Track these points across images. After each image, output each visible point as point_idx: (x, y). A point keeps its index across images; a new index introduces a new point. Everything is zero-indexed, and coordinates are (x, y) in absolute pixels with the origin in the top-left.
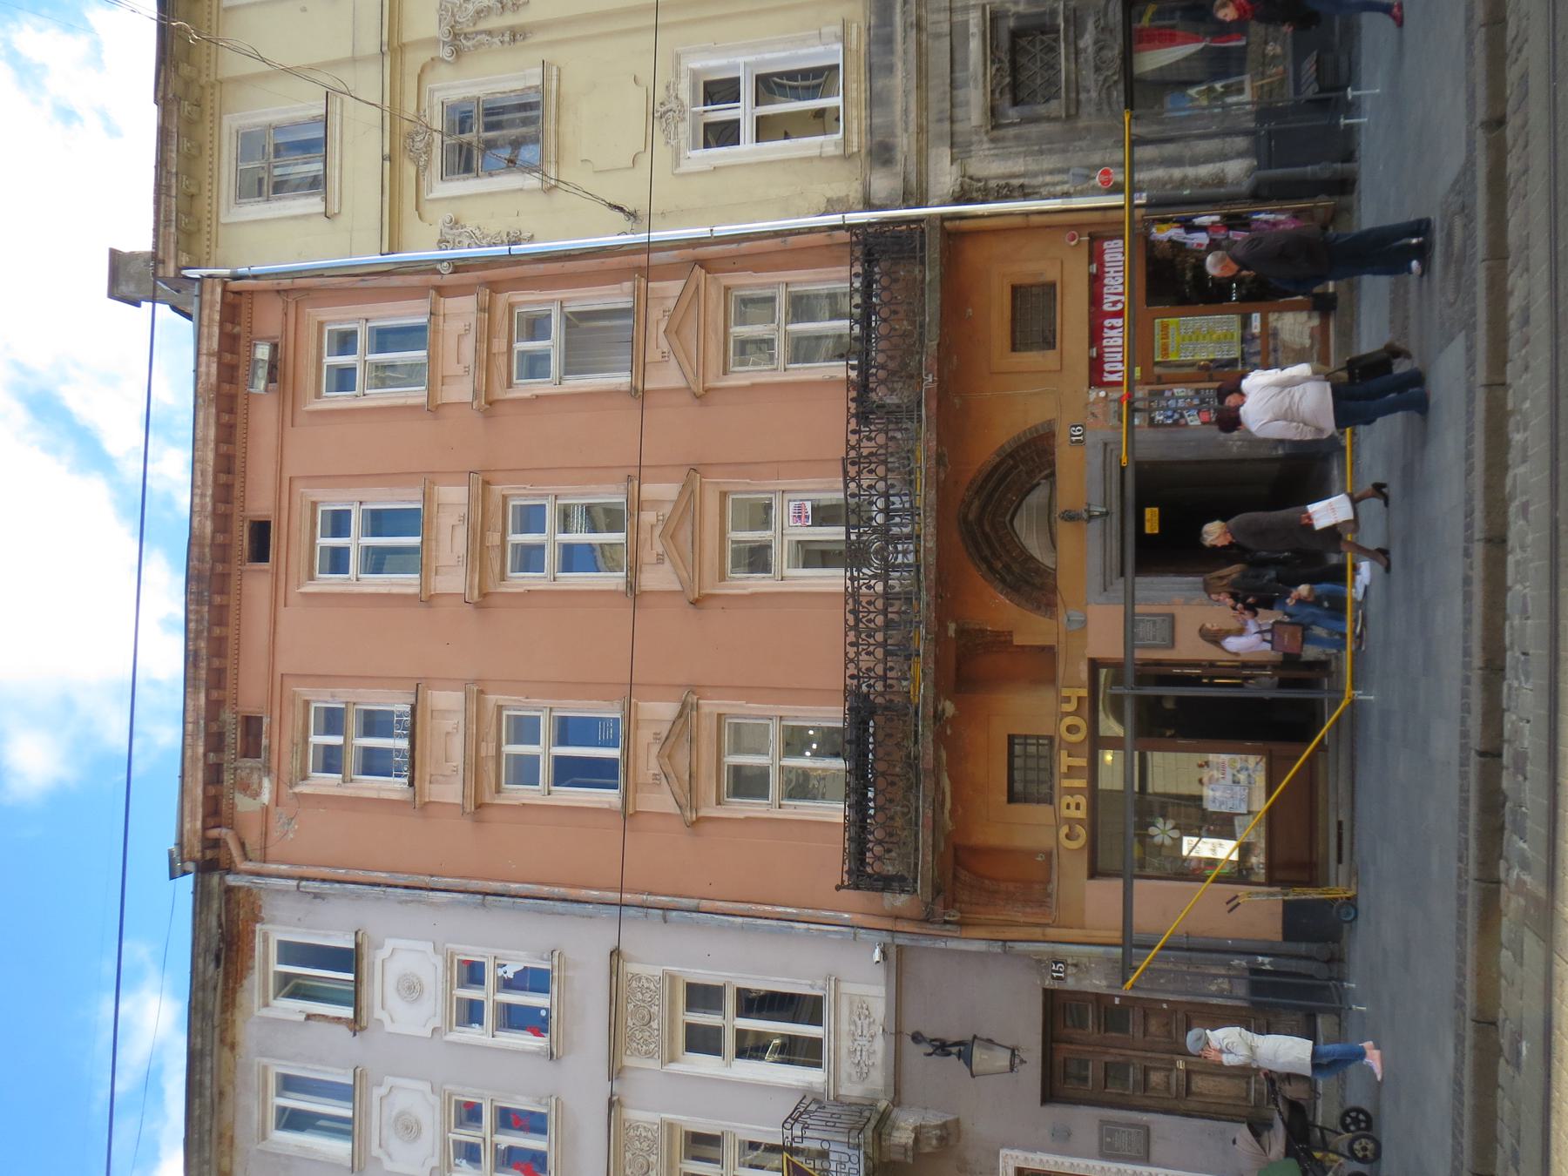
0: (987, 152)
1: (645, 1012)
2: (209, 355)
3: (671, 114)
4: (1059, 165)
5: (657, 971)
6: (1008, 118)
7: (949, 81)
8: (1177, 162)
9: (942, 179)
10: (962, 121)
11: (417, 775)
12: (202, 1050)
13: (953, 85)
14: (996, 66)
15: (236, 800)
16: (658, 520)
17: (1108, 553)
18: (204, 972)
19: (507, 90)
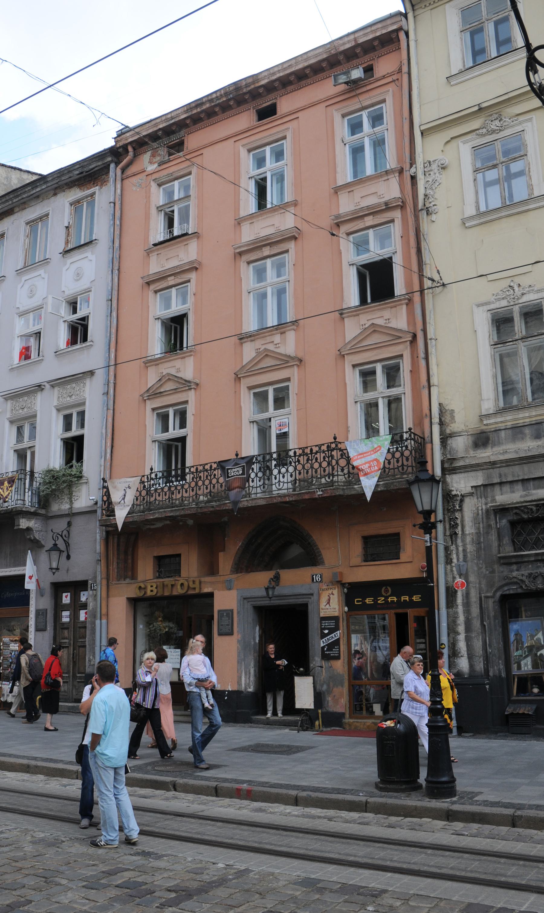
0: (480, 508)
1: (72, 393)
2: (355, 40)
3: (512, 291)
4: (469, 555)
5: (87, 395)
6: (500, 519)
7: (526, 478)
8: (468, 628)
9: (462, 482)
10: (501, 489)
11: (159, 247)
12: (48, 181)
13: (524, 481)
14: (534, 508)
15: (148, 153)
16: (276, 344)
17: (261, 599)
18: (74, 170)
19: (531, 174)
